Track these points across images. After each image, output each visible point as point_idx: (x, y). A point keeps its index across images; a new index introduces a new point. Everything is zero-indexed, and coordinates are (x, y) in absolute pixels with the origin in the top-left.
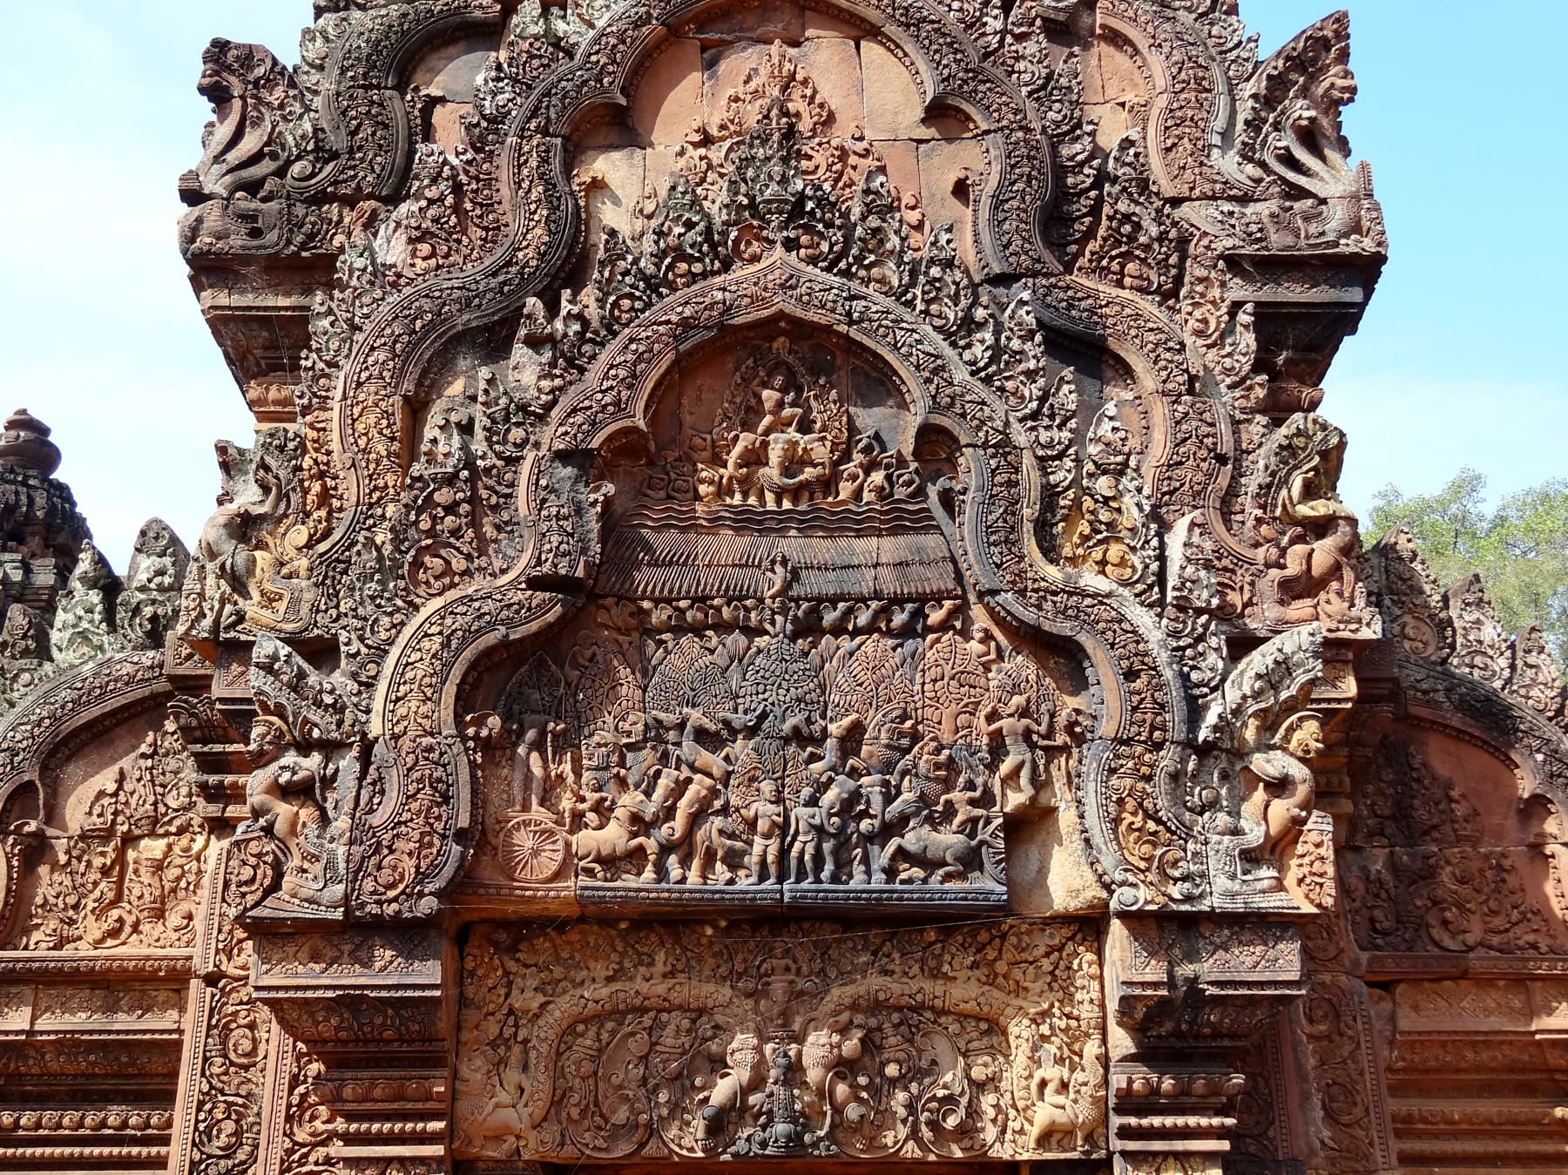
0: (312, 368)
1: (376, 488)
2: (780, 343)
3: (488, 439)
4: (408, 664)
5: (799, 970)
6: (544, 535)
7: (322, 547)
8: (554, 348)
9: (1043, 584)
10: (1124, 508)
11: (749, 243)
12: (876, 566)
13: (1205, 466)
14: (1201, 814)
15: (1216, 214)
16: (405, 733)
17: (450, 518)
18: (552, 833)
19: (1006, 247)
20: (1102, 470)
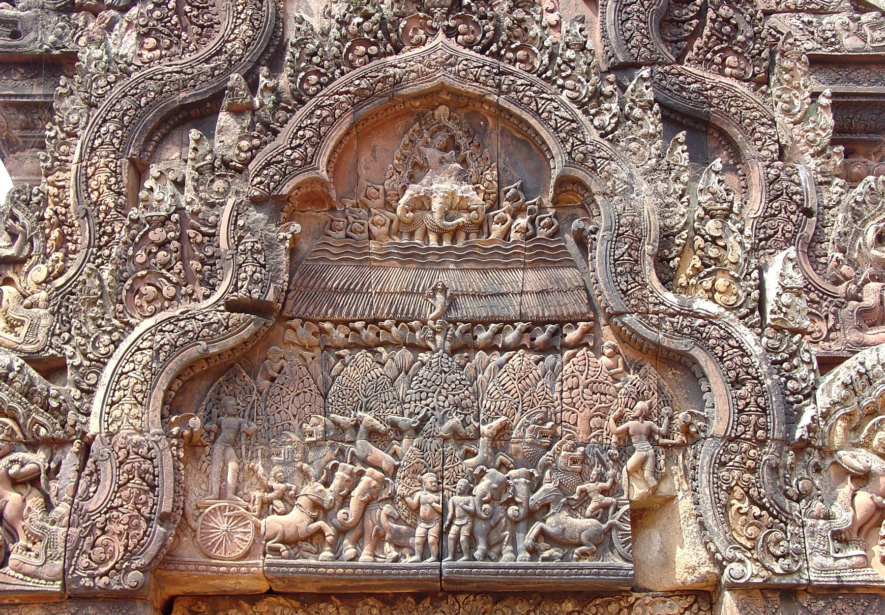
0: (55, 137)
1: (104, 233)
2: (442, 111)
3: (196, 189)
4: (122, 373)
6: (240, 266)
7: (60, 282)
8: (253, 114)
9: (662, 307)
10: (729, 245)
11: (415, 30)
12: (521, 293)
13: (794, 218)
14: (798, 501)
15: (798, 23)
16: (118, 432)
17: (162, 253)
18: (244, 518)
19: (628, 41)
20: (710, 214)
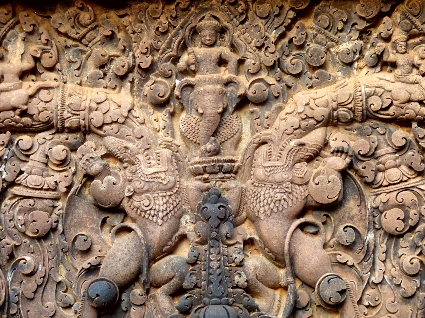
5: (241, 62)
